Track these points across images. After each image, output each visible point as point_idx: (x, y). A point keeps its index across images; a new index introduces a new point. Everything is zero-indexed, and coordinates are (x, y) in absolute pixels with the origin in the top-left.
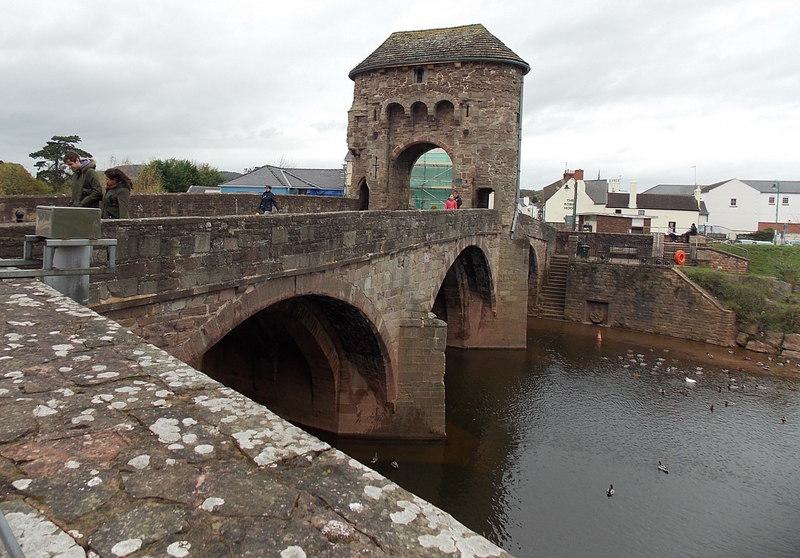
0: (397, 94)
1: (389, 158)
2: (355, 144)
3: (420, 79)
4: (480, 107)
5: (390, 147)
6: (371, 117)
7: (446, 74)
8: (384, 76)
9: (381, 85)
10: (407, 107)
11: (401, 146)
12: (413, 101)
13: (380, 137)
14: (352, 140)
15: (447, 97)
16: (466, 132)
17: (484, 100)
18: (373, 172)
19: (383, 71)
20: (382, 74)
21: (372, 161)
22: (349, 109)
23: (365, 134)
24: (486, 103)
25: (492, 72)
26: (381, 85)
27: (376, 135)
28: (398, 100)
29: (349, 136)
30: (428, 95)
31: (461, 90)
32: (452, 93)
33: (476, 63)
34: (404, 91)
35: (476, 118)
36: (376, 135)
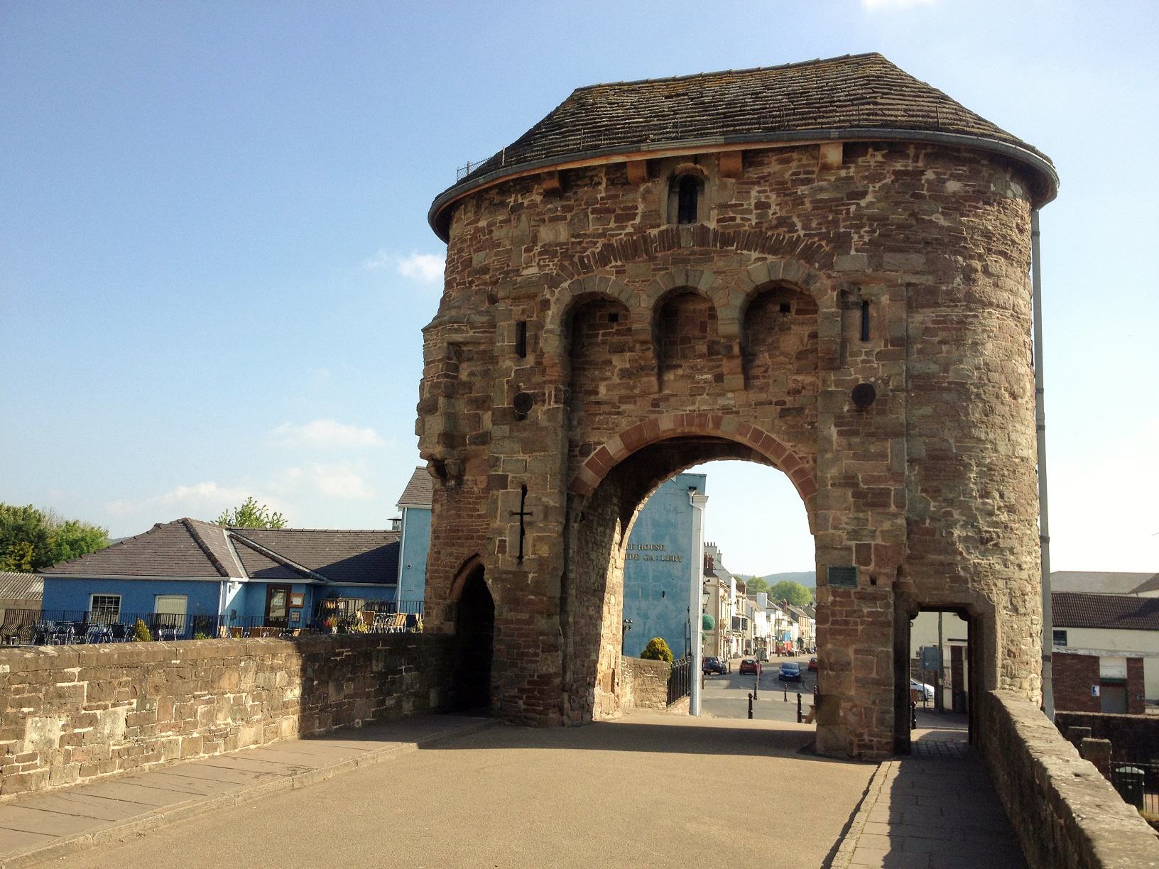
0: (603, 259)
1: (571, 488)
2: (450, 438)
3: (687, 211)
4: (911, 306)
5: (575, 450)
6: (506, 341)
7: (782, 189)
8: (559, 204)
9: (546, 234)
10: (642, 307)
11: (615, 448)
12: (663, 284)
13: (539, 412)
14: (437, 424)
15: (792, 271)
16: (863, 396)
17: (928, 280)
18: (510, 538)
19: (555, 183)
20: (549, 194)
21: (507, 498)
22: (428, 320)
23: (482, 403)
24: (932, 291)
25: (953, 186)
26: (546, 234)
27: (523, 404)
28: (607, 281)
29: (425, 409)
30: (720, 263)
31: (841, 243)
32: (809, 254)
33: (894, 149)
34: (631, 250)
35: (902, 343)
36: (523, 404)
